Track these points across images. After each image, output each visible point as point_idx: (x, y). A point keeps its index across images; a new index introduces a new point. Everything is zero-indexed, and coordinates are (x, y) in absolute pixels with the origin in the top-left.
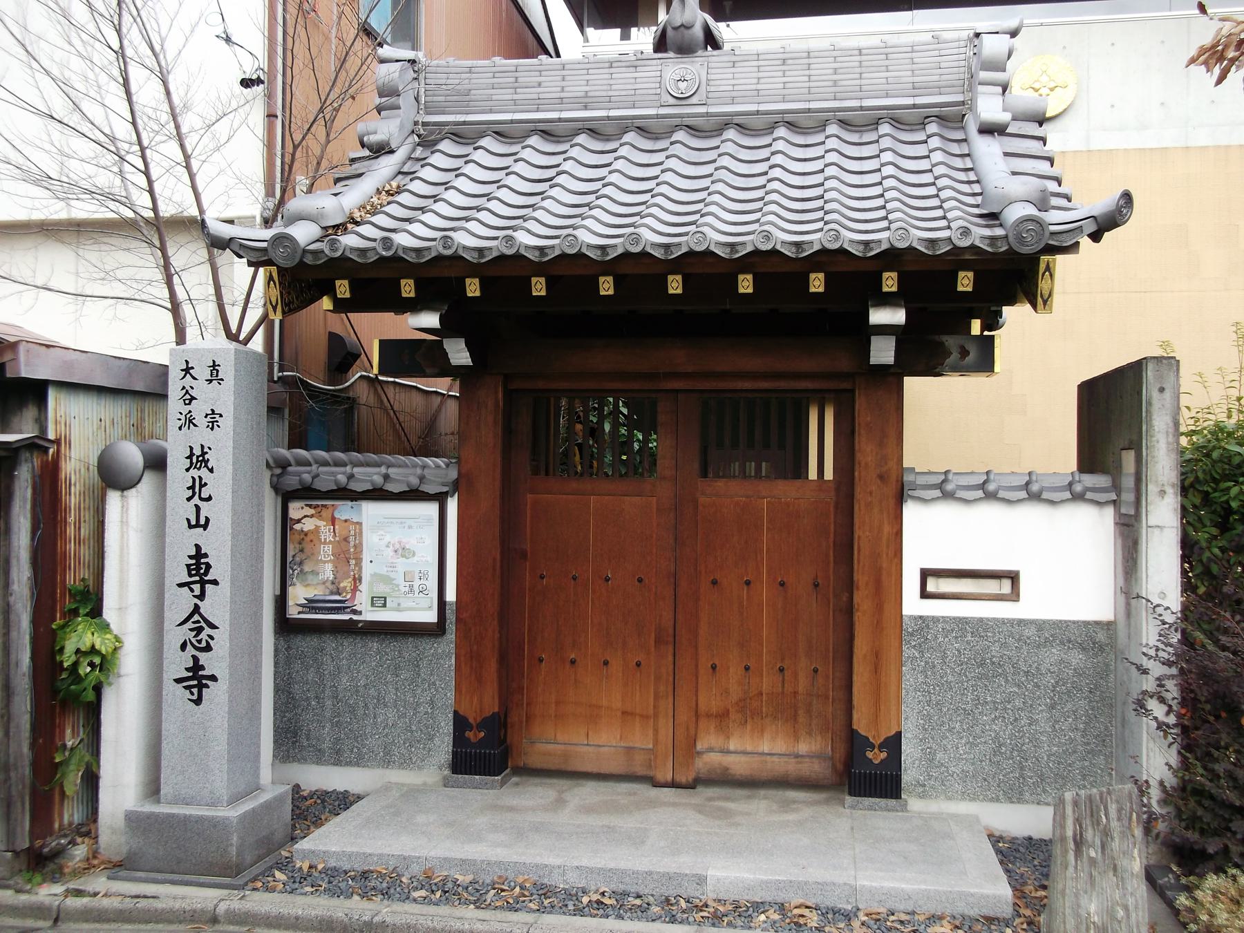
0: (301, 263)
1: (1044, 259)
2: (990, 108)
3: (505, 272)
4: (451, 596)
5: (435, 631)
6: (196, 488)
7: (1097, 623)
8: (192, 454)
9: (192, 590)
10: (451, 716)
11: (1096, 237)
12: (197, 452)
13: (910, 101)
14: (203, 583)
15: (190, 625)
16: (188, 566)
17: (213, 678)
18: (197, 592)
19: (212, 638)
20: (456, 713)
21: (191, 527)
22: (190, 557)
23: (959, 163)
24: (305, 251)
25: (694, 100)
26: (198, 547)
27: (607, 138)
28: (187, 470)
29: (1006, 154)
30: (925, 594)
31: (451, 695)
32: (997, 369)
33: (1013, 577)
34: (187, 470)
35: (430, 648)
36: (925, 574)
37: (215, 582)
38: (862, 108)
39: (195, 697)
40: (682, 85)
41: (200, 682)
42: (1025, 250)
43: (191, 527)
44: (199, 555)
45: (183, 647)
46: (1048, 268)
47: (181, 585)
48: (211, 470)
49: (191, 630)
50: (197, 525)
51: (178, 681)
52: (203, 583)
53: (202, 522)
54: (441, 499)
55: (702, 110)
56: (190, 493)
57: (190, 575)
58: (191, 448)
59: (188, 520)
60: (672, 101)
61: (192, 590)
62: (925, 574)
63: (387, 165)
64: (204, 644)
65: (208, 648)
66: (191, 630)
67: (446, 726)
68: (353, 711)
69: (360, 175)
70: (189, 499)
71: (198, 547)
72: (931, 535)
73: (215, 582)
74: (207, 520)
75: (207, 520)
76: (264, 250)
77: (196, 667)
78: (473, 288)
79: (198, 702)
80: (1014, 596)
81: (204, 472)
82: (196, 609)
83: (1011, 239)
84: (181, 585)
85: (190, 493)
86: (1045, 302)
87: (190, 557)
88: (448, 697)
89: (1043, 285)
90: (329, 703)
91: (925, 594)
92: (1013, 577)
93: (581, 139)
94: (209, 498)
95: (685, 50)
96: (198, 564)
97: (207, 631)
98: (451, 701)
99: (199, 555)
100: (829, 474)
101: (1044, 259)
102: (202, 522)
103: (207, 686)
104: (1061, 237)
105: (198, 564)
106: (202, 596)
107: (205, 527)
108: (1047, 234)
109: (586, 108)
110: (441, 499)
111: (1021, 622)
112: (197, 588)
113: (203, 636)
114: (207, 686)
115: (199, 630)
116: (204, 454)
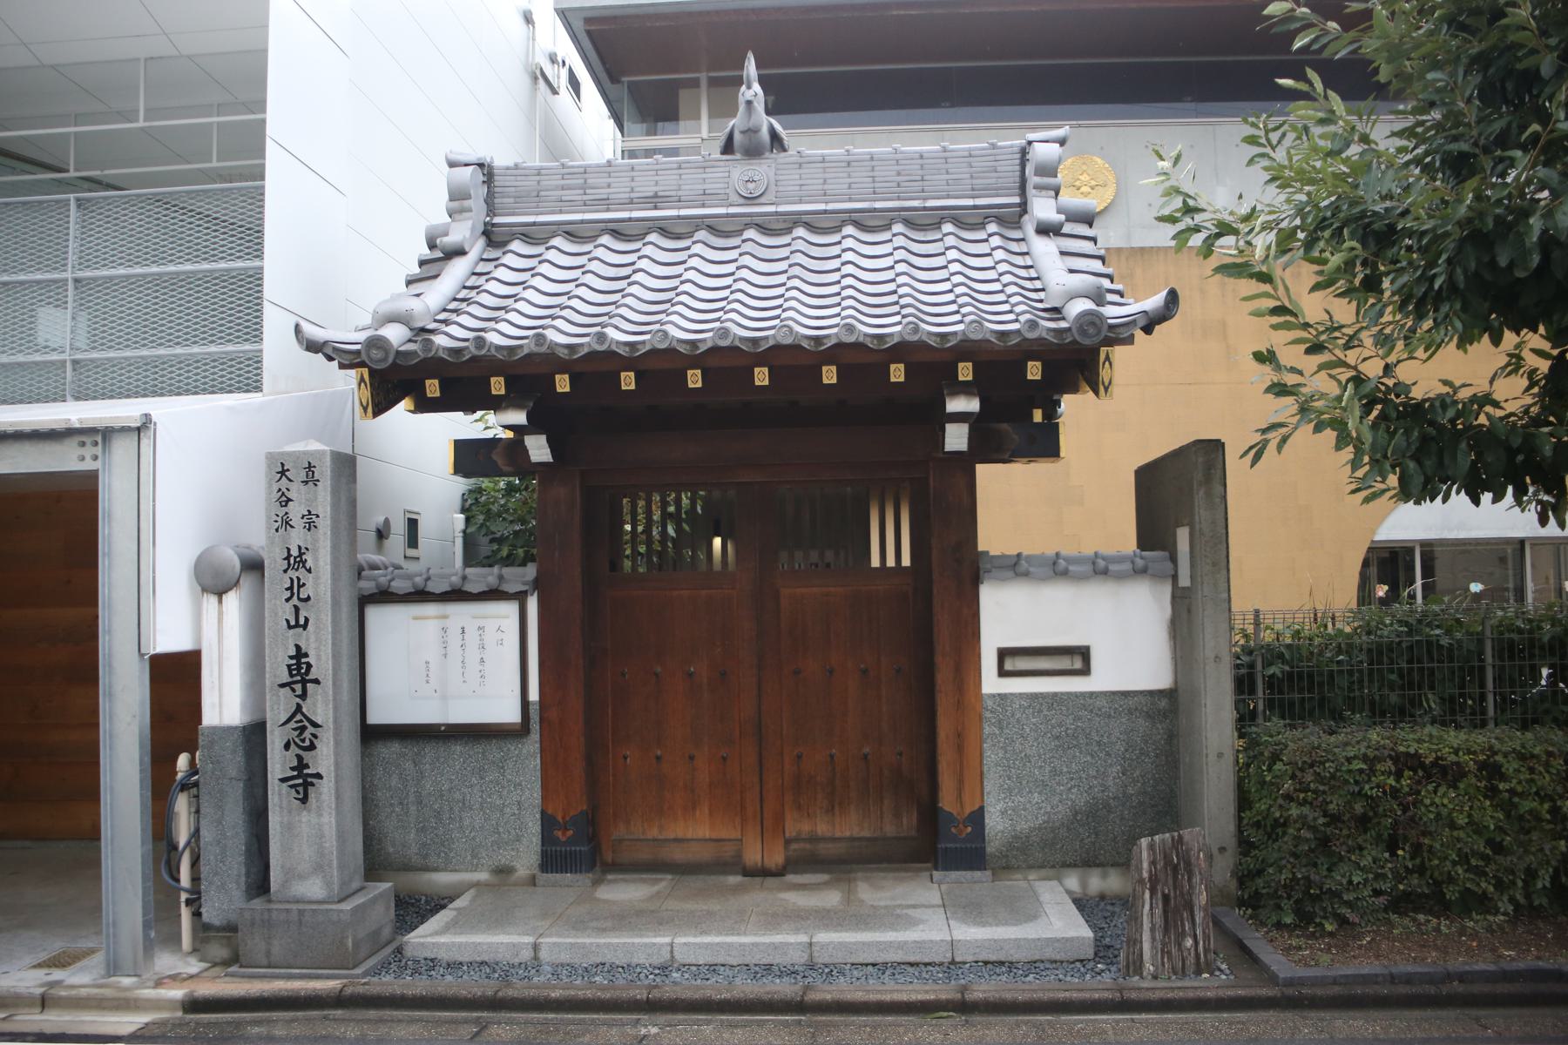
0: (394, 364)
1: (1103, 350)
2: (1043, 208)
3: (595, 367)
4: (534, 695)
5: (517, 732)
6: (294, 588)
7: (1161, 692)
9: (293, 690)
10: (538, 816)
11: (1148, 330)
12: (295, 552)
13: (970, 202)
14: (304, 682)
15: (293, 724)
16: (289, 666)
17: (318, 776)
18: (299, 692)
19: (315, 736)
20: (543, 813)
21: (290, 627)
22: (291, 657)
23: (1019, 260)
24: (398, 352)
25: (762, 200)
26: (298, 647)
27: (678, 237)
29: (1062, 253)
30: (1003, 673)
31: (537, 794)
32: (1062, 454)
33: (1084, 653)
35: (512, 748)
36: (1003, 654)
37: (316, 681)
38: (925, 209)
40: (751, 186)
42: (1087, 342)
43: (290, 627)
44: (300, 654)
45: (287, 746)
46: (1107, 358)
47: (282, 686)
48: (309, 571)
50: (297, 625)
53: (302, 621)
54: (521, 597)
55: (772, 209)
56: (288, 594)
57: (291, 675)
60: (742, 201)
61: (293, 690)
62: (1003, 654)
63: (457, 270)
64: (307, 743)
65: (312, 747)
67: (534, 827)
68: (438, 814)
69: (436, 277)
70: (287, 600)
71: (298, 647)
72: (1007, 615)
73: (316, 681)
74: (307, 620)
75: (307, 620)
76: (358, 352)
77: (301, 765)
78: (563, 384)
79: (304, 800)
80: (1085, 671)
81: (302, 573)
82: (299, 708)
83: (1074, 330)
84: (282, 686)
85: (288, 594)
86: (1106, 389)
87: (291, 657)
88: (533, 794)
89: (1104, 374)
90: (413, 808)
91: (1003, 673)
92: (1084, 653)
93: (653, 237)
94: (309, 598)
95: (753, 152)
96: (299, 664)
97: (311, 729)
98: (538, 801)
99: (300, 654)
100: (906, 561)
101: (1103, 350)
102: (302, 621)
105: (299, 664)
106: (304, 696)
107: (305, 627)
108: (1105, 328)
109: (656, 208)
110: (521, 597)
111: (1092, 694)
112: (298, 687)
113: (307, 734)
114: (312, 784)
115: (303, 729)
116: (301, 554)
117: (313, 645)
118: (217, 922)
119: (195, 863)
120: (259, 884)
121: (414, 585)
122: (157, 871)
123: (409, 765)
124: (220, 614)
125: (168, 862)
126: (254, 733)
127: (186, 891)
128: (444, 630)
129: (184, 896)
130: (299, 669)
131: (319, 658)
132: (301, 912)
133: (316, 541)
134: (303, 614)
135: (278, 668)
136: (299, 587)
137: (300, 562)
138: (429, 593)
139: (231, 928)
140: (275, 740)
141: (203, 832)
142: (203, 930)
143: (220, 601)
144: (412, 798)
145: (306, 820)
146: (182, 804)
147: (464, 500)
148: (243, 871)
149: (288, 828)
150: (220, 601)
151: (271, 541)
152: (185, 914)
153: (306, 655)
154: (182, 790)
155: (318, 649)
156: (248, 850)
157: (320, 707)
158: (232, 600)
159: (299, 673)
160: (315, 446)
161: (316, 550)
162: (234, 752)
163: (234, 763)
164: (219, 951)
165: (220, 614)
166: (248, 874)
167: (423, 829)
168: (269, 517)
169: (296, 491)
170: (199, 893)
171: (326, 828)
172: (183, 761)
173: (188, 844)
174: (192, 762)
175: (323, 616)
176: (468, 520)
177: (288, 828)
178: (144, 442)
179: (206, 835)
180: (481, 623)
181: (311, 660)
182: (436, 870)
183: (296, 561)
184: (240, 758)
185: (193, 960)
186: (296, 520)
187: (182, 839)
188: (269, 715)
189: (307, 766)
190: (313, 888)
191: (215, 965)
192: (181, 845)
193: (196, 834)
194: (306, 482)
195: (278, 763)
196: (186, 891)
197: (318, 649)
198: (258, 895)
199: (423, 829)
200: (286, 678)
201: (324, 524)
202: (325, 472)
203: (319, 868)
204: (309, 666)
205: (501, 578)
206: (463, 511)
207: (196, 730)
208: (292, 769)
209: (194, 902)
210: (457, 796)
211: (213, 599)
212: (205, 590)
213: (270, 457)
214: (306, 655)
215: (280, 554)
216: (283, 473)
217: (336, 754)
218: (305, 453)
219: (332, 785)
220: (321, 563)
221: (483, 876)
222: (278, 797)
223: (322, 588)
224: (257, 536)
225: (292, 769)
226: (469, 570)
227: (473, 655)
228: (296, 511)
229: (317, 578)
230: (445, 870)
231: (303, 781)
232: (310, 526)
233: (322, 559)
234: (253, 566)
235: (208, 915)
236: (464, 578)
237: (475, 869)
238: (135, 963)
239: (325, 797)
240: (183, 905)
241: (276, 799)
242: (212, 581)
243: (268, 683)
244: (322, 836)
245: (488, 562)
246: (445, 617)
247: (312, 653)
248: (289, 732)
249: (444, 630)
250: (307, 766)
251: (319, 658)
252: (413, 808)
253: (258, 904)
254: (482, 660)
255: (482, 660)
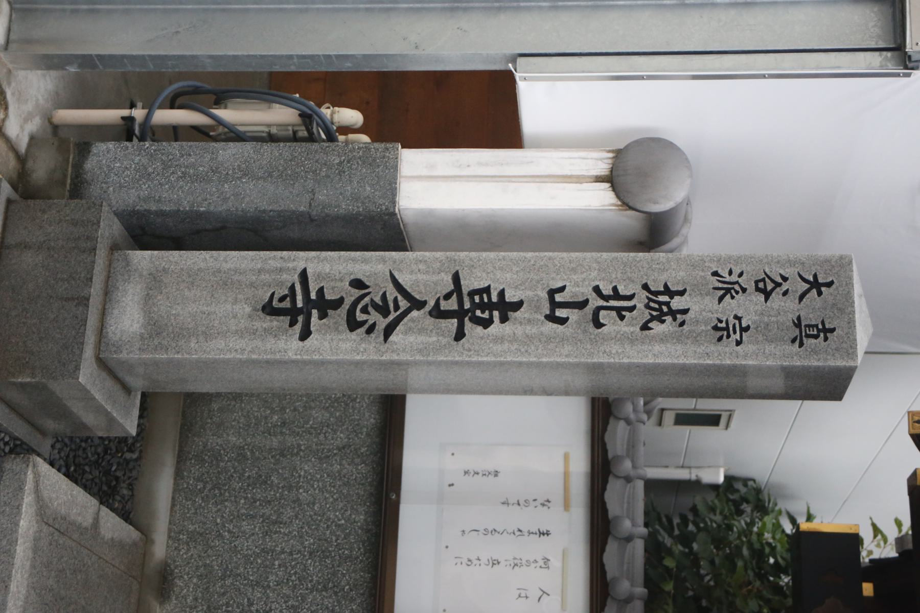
6: (616, 301)
8: (667, 291)
9: (447, 297)
12: (677, 303)
14: (460, 314)
15: (392, 293)
16: (487, 290)
18: (444, 305)
19: (370, 331)
21: (552, 293)
26: (518, 305)
28: (645, 287)
34: (645, 287)
37: (460, 335)
39: (275, 303)
41: (300, 311)
43: (552, 293)
44: (506, 308)
45: (358, 284)
47: (456, 278)
48: (645, 327)
49: (384, 296)
50: (554, 305)
51: (304, 275)
52: (460, 314)
53: (560, 313)
56: (607, 290)
57: (472, 294)
58: (682, 293)
59: (562, 289)
61: (447, 297)
64: (360, 317)
65: (353, 325)
66: (384, 296)
70: (597, 290)
71: (518, 305)
73: (460, 335)
74: (563, 321)
75: (563, 321)
77: (325, 306)
79: (269, 309)
82: (418, 305)
84: (456, 278)
85: (607, 290)
87: (502, 293)
90: (275, 442)
94: (598, 325)
96: (490, 306)
97: (382, 323)
99: (506, 308)
102: (560, 313)
103: (292, 324)
105: (490, 306)
106: (438, 313)
107: (552, 318)
112: (452, 305)
113: (374, 317)
114: (292, 324)
115: (384, 310)
117: (519, 330)
118: (90, 164)
119: (199, 133)
120: (147, 232)
121: (618, 458)
122: (181, 76)
123: (341, 437)
124: (579, 179)
125: (196, 91)
126: (385, 231)
127: (148, 117)
128: (546, 503)
129: (138, 114)
130: (483, 306)
131: (499, 340)
132: (84, 301)
133: (696, 338)
134: (573, 315)
135: (486, 271)
136: (619, 310)
137: (661, 313)
138: (605, 482)
139: (77, 188)
140: (372, 265)
141: (233, 148)
142: (80, 142)
143: (599, 179)
144: (290, 440)
145: (237, 310)
146: (281, 115)
147: (745, 481)
148: (166, 208)
149: (226, 283)
150: (599, 179)
151: (695, 264)
152: (112, 115)
153: (504, 319)
154: (302, 115)
155: (514, 339)
156: (200, 215)
157: (417, 339)
158: (600, 198)
159: (475, 306)
160: (863, 337)
161: (679, 339)
162: (356, 198)
163: (338, 196)
164: (42, 168)
165: (579, 179)
166: (161, 213)
167: (241, 458)
168: (738, 260)
169: (784, 307)
170: (142, 139)
171: (220, 343)
172: (351, 116)
173: (219, 122)
174: (346, 130)
175: (567, 349)
176: (715, 487)
177: (226, 283)
178: (875, 59)
179: (228, 152)
180: (556, 563)
181: (496, 328)
182: (178, 474)
183: (662, 306)
184: (345, 207)
185: (34, 125)
186: (732, 306)
187: (229, 114)
188: (409, 254)
189: (323, 315)
190: (128, 319)
191: (22, 160)
192: (220, 113)
193: (234, 135)
194: (798, 324)
195: (332, 269)
196: (148, 117)
197: (514, 339)
198: (128, 228)
199: (241, 458)
200: (468, 285)
201: (725, 355)
202: (817, 357)
203: (156, 329)
204: (486, 323)
205: (629, 539)
206: (729, 479)
207: (396, 140)
208: (321, 291)
209: (126, 131)
210: (289, 513)
211: (602, 168)
212: (618, 154)
213: (843, 264)
214: (504, 319)
215: (675, 278)
216: (815, 285)
217: (339, 363)
218: (851, 323)
219: (291, 355)
220: (657, 348)
221: (160, 549)
222: (280, 267)
223: (615, 348)
224: (707, 237)
225: (321, 291)
226: (640, 485)
227: (505, 548)
228: (748, 307)
229: (632, 340)
230: (176, 489)
231: (297, 309)
232: (721, 331)
233: (664, 350)
234: (655, 233)
235: (104, 153)
236: (628, 479)
237: (172, 536)
238: (28, 41)
239: (271, 343)
240: (125, 112)
241: (273, 264)
242: (631, 166)
243: (463, 255)
244: (207, 336)
245: (652, 516)
246: (567, 506)
247: (507, 328)
248: (381, 287)
249: (546, 503)
250: (323, 315)
251: (499, 340)
252: (275, 442)
253: (110, 228)
254: (495, 563)
255: (495, 563)
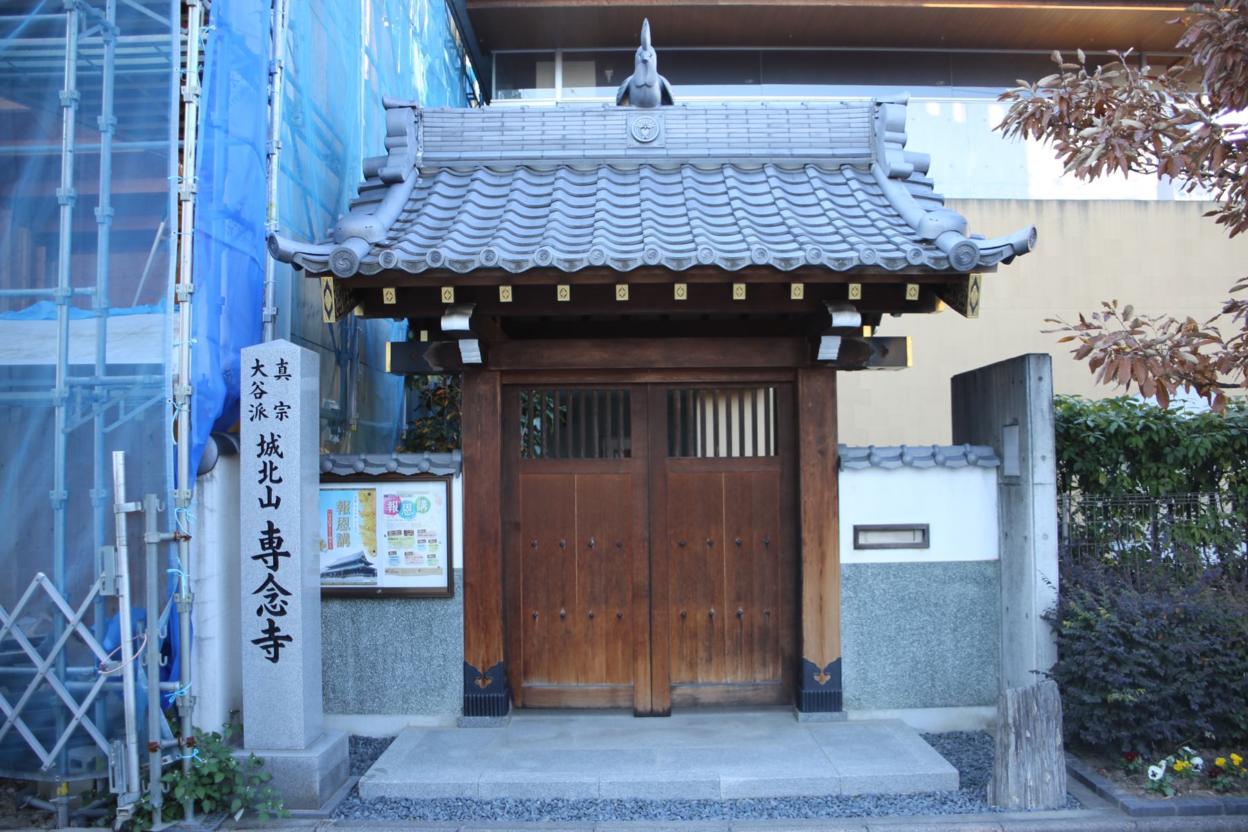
0: (358, 274)
1: (973, 275)
2: (895, 159)
3: (536, 283)
4: (458, 563)
5: (446, 594)
6: (267, 472)
7: (987, 562)
8: (261, 444)
9: (266, 562)
10: (461, 667)
11: (1007, 261)
12: (268, 439)
13: (830, 152)
14: (276, 555)
15: (265, 592)
16: (262, 541)
17: (288, 638)
18: (271, 563)
19: (286, 603)
20: (465, 663)
21: (263, 506)
22: (264, 533)
23: (877, 201)
24: (361, 263)
25: (655, 144)
26: (270, 524)
28: (259, 456)
29: (914, 196)
30: (857, 546)
31: (461, 649)
32: (910, 363)
33: (924, 530)
34: (259, 456)
35: (438, 606)
36: (858, 530)
37: (287, 554)
38: (792, 156)
39: (272, 656)
40: (645, 132)
41: (276, 642)
42: (962, 269)
43: (263, 506)
44: (271, 530)
45: (260, 612)
46: (975, 283)
47: (256, 558)
48: (281, 456)
49: (266, 597)
50: (269, 504)
51: (256, 642)
52: (276, 555)
53: (274, 501)
54: (447, 479)
55: (664, 152)
56: (262, 476)
57: (264, 549)
58: (262, 437)
59: (261, 500)
60: (637, 144)
61: (266, 562)
62: (858, 530)
63: (399, 195)
64: (278, 609)
66: (266, 597)
67: (458, 677)
68: (373, 666)
69: (380, 201)
70: (261, 482)
71: (270, 524)
72: (862, 497)
73: (287, 554)
74: (278, 499)
75: (278, 499)
76: (326, 263)
77: (272, 629)
78: (506, 295)
79: (275, 659)
80: (925, 544)
81: (274, 458)
82: (271, 578)
83: (952, 260)
84: (256, 558)
85: (262, 476)
86: (973, 309)
87: (264, 533)
88: (457, 649)
89: (972, 296)
91: (857, 546)
92: (924, 530)
93: (562, 173)
94: (280, 480)
95: (646, 104)
97: (281, 597)
98: (461, 654)
99: (271, 530)
100: (761, 452)
101: (973, 275)
102: (274, 501)
103: (283, 646)
104: (987, 259)
106: (275, 567)
107: (276, 505)
108: (978, 257)
109: (564, 148)
110: (447, 479)
111: (931, 564)
112: (270, 560)
113: (278, 601)
114: (283, 646)
115: (274, 596)
116: (273, 441)
123: (348, 622)
130: (271, 543)
136: (272, 470)
144: (350, 651)
167: (360, 678)
186: (271, 412)
199: (360, 678)
